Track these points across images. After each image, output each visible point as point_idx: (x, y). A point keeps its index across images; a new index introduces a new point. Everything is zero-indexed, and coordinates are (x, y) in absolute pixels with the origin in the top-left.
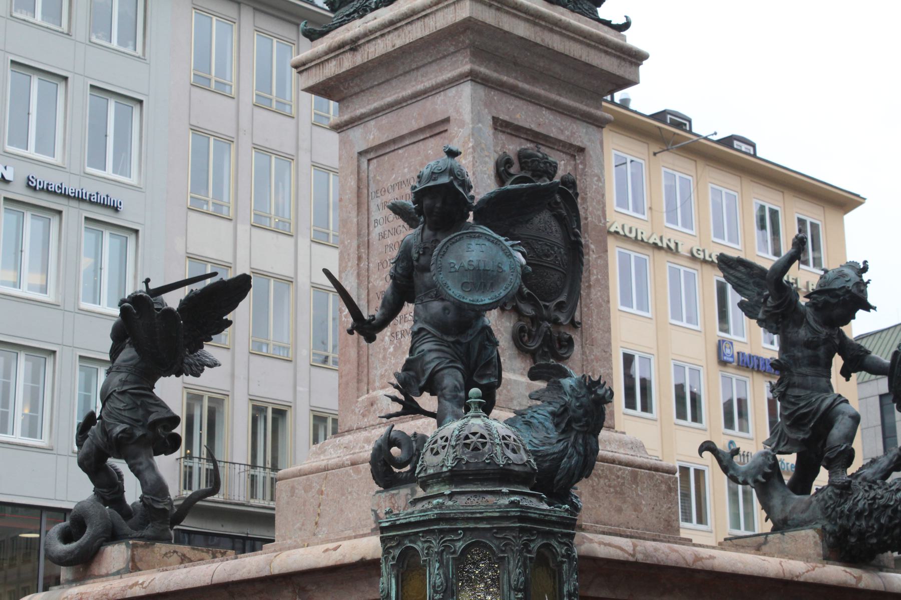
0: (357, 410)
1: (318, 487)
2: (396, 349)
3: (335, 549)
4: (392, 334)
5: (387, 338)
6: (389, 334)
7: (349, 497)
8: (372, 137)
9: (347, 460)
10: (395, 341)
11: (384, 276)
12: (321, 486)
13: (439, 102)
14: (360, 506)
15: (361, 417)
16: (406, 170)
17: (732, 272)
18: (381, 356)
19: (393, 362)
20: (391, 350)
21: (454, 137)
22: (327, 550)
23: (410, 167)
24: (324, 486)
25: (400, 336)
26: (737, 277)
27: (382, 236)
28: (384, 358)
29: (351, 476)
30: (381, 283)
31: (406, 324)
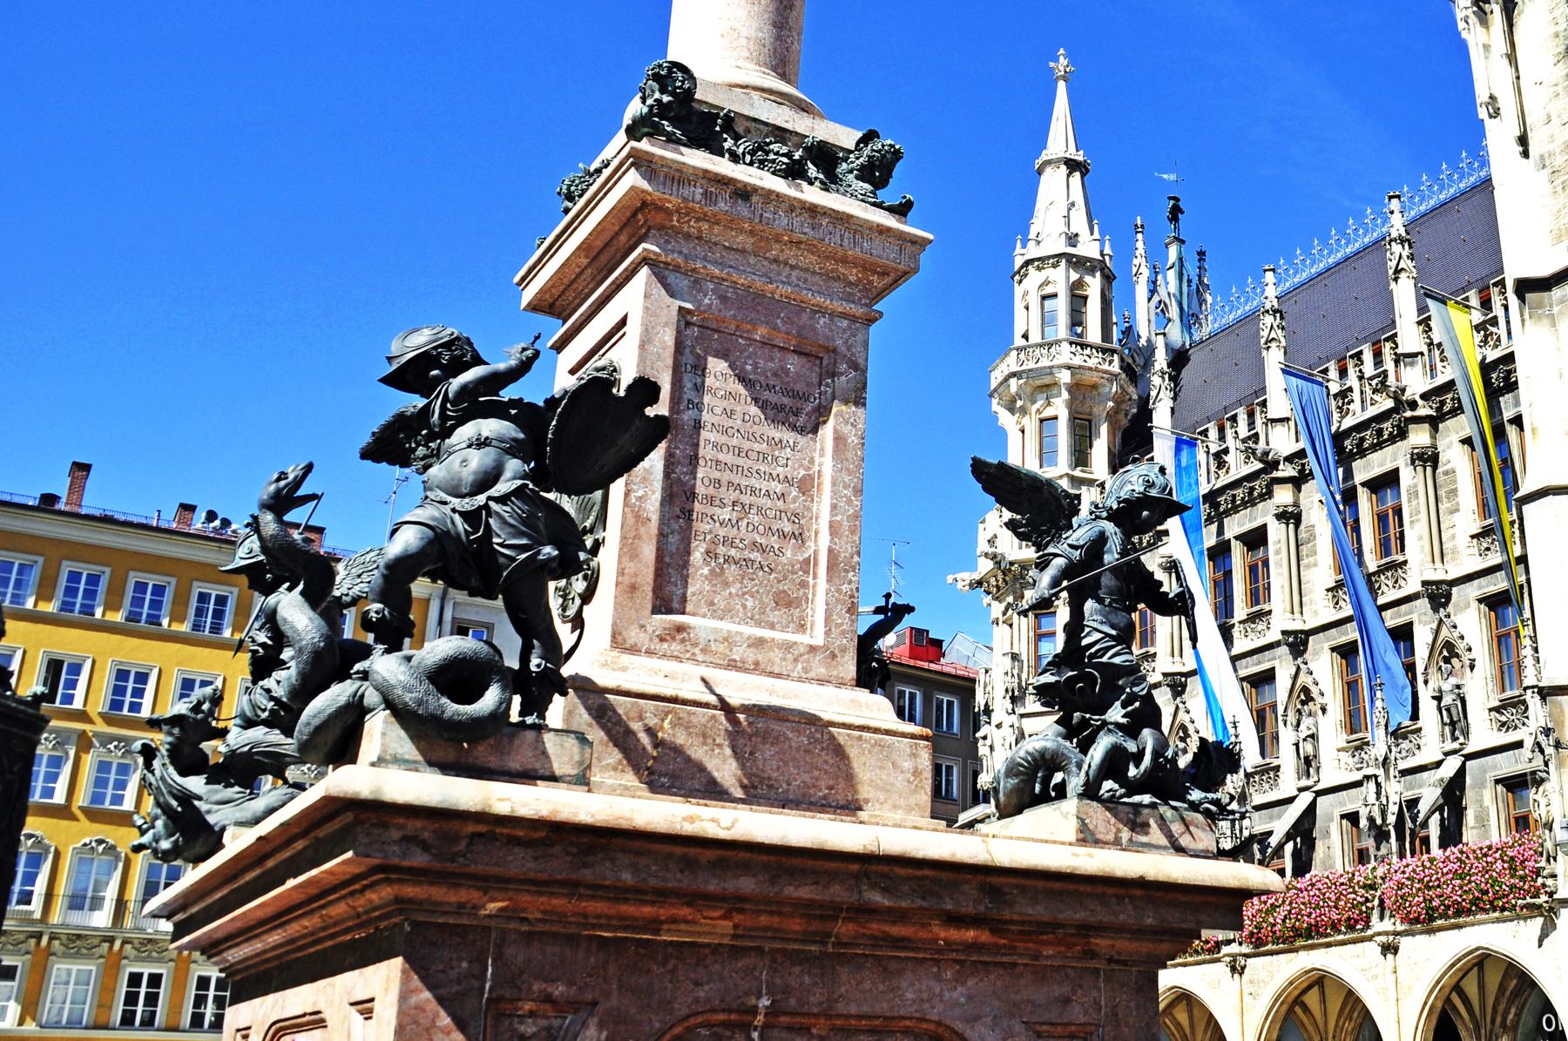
2: (712, 571)
4: (708, 552)
6: (703, 550)
7: (717, 751)
8: (706, 301)
12: (663, 720)
19: (708, 588)
20: (706, 571)
24: (667, 721)
25: (722, 560)
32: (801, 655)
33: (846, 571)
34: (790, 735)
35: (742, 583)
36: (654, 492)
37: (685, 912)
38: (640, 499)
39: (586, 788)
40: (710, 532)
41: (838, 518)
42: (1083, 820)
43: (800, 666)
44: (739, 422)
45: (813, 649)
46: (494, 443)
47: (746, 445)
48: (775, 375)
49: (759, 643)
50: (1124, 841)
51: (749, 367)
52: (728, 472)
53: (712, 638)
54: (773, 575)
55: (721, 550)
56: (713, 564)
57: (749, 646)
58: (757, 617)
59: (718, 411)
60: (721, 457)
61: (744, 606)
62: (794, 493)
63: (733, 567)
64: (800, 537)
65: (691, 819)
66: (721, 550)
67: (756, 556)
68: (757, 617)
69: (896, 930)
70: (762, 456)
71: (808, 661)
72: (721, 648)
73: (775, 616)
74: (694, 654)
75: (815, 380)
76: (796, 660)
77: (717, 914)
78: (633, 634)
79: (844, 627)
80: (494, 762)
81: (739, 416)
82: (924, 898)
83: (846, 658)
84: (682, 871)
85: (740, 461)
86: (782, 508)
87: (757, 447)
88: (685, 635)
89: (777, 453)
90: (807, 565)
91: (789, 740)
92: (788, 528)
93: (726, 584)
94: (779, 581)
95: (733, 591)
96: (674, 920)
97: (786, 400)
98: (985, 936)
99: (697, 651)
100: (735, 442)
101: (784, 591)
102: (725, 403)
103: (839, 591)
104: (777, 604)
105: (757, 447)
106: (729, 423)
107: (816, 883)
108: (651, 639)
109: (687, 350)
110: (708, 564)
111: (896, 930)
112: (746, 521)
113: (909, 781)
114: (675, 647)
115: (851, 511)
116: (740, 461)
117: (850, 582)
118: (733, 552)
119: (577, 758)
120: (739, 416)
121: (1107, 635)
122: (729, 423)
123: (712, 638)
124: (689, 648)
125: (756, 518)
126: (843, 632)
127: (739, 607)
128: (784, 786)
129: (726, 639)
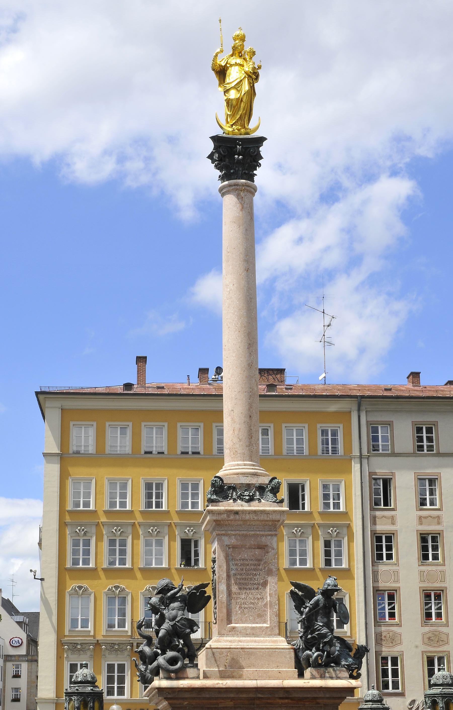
0: (227, 629)
1: (226, 654)
3: (309, 682)
5: (237, 608)
6: (238, 607)
7: (241, 659)
8: (233, 541)
9: (239, 647)
10: (241, 610)
11: (236, 588)
12: (228, 654)
13: (263, 539)
14: (245, 662)
15: (228, 632)
16: (246, 556)
17: (293, 595)
18: (235, 613)
20: (239, 612)
21: (270, 552)
22: (305, 683)
23: (248, 555)
26: (294, 597)
27: (235, 575)
28: (236, 614)
29: (241, 652)
30: (234, 590)
31: (246, 605)
32: (264, 630)
33: (275, 606)
34: (258, 653)
35: (248, 613)
36: (224, 595)
37: (222, 701)
38: (221, 598)
39: (199, 679)
40: (240, 602)
41: (271, 592)
42: (312, 673)
43: (264, 633)
44: (245, 571)
45: (267, 627)
46: (176, 608)
47: (247, 577)
48: (253, 556)
49: (253, 628)
50: (323, 676)
51: (246, 556)
52: (243, 585)
53: (242, 629)
54: (256, 610)
55: (243, 606)
56: (241, 610)
57: (251, 630)
58: (253, 621)
59: (239, 570)
60: (241, 582)
61: (250, 619)
62: (260, 587)
63: (246, 609)
64: (262, 598)
65: (218, 684)
66: (243, 606)
67: (252, 606)
68: (253, 621)
69: (269, 701)
70: (251, 579)
71: (266, 631)
72: (244, 631)
73: (257, 620)
74: (238, 634)
75: (264, 555)
76: (263, 631)
77: (229, 701)
78: (223, 631)
79: (275, 621)
80: (182, 676)
81: (244, 570)
82: (271, 695)
83: (276, 628)
84: (218, 694)
85: (246, 582)
86: (257, 592)
87: (250, 577)
88: (235, 629)
89: (255, 577)
90: (266, 605)
91: (258, 654)
92: (259, 597)
93: (245, 614)
94: (258, 611)
95: (247, 616)
96: (221, 703)
97: (256, 562)
98: (290, 701)
99: (238, 633)
100: (244, 577)
101: (259, 613)
102: (241, 567)
103: (273, 611)
104: (258, 617)
105: (250, 577)
106: (243, 572)
107: (246, 694)
108: (227, 632)
109: (230, 555)
110: (240, 610)
111: (269, 701)
112: (248, 597)
113: (288, 660)
114: (233, 633)
115: (275, 589)
116: (246, 582)
117: (276, 609)
118: (246, 606)
119: (197, 673)
120: (244, 570)
121: (320, 625)
122: (243, 572)
123: (242, 629)
124: (236, 632)
125: (251, 596)
126: (275, 622)
127: (248, 620)
128: (257, 665)
129: (245, 629)
